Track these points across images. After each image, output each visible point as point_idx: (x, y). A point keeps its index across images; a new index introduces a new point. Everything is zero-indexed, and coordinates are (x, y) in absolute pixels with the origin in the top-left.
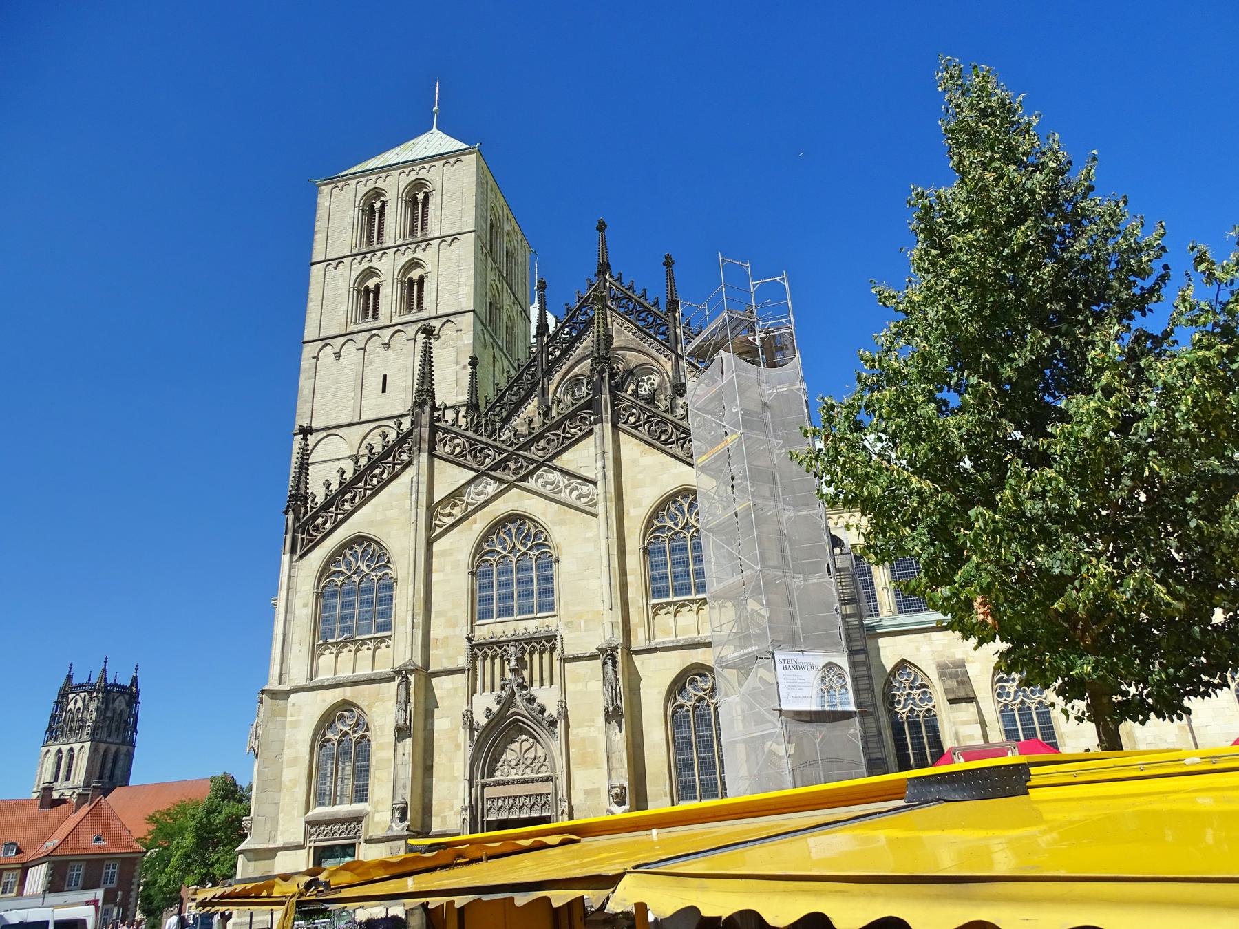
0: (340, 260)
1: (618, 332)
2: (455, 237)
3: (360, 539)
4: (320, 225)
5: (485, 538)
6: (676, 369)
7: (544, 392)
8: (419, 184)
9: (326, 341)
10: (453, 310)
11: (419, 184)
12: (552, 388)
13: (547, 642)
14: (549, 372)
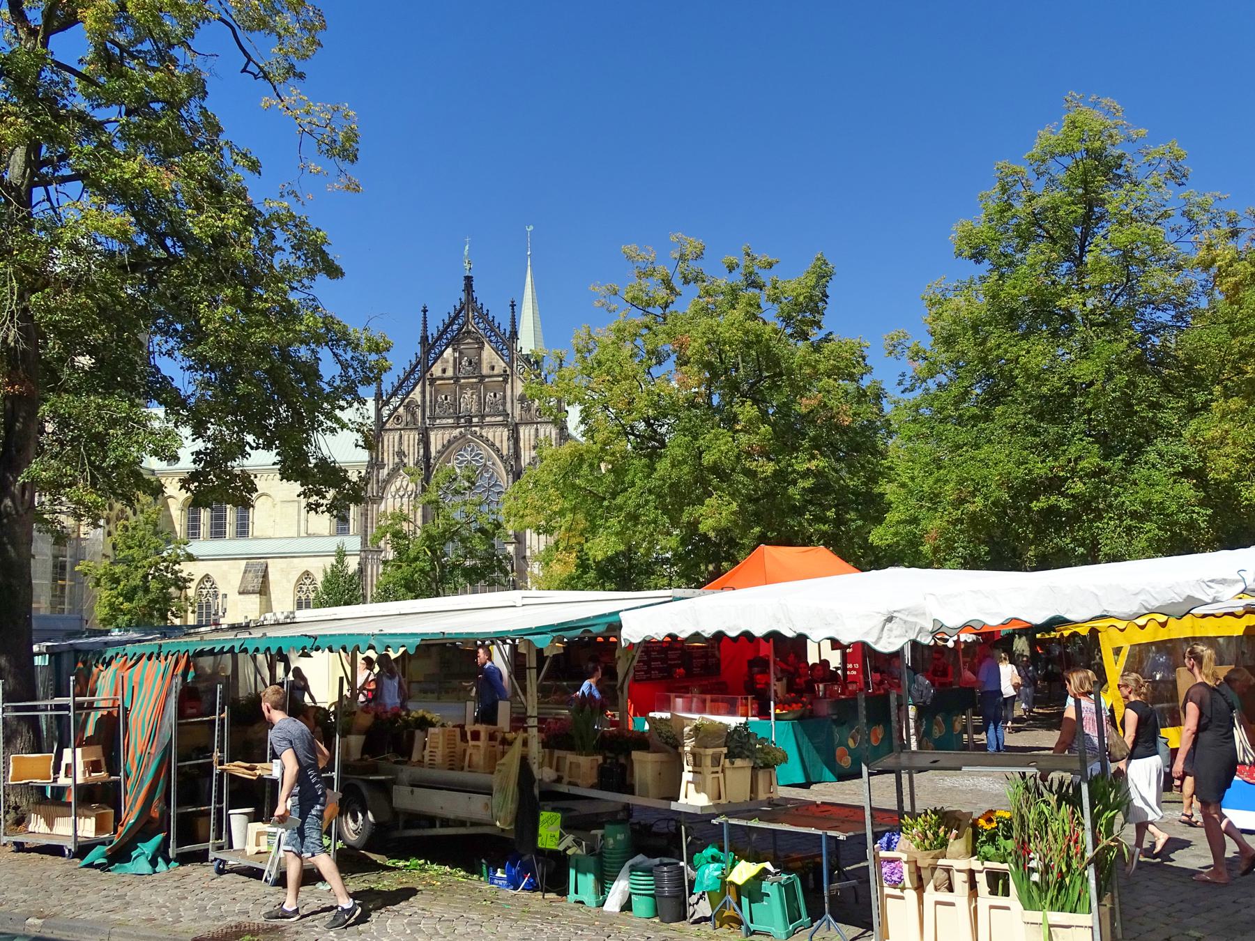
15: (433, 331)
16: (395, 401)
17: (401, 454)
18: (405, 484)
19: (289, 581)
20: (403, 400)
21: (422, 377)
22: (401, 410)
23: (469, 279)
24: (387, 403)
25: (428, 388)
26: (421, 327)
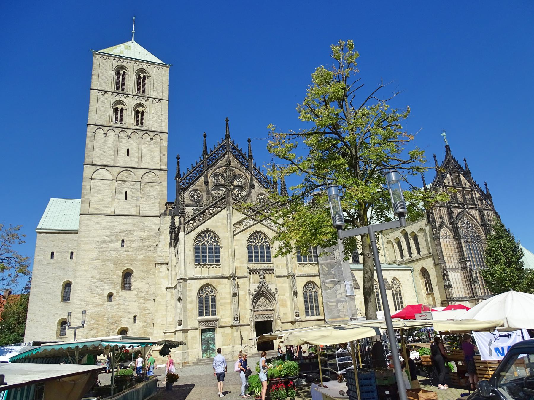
0: (106, 92)
1: (233, 161)
2: (160, 100)
3: (207, 231)
4: (94, 72)
6: (252, 179)
7: (206, 176)
8: (142, 71)
9: (100, 126)
10: (159, 130)
11: (142, 71)
12: (209, 175)
13: (270, 271)
14: (208, 169)
17: (441, 218)
18: (445, 232)
23: (447, 147)
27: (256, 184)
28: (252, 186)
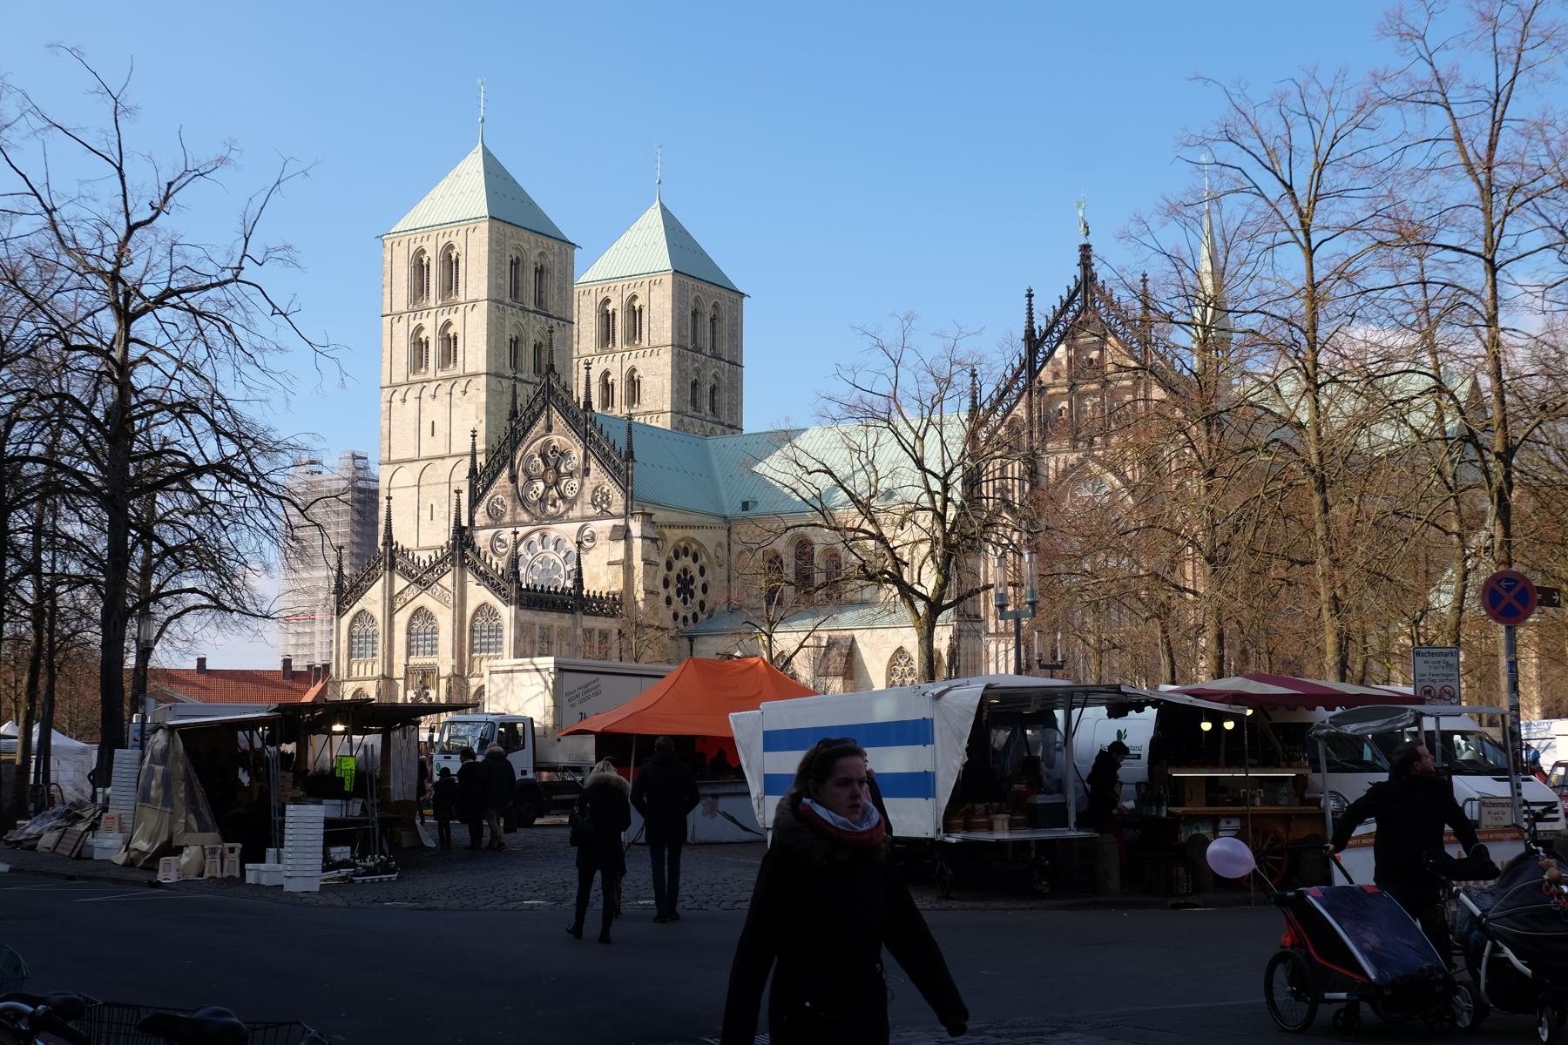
0: (400, 315)
5: (412, 617)
7: (512, 466)
15: (1040, 323)
16: (994, 419)
19: (880, 660)
20: (1003, 420)
21: (1029, 387)
22: (1002, 431)
23: (1086, 248)
24: (984, 423)
25: (1035, 399)
26: (1025, 318)
27: (593, 466)
28: (587, 471)
